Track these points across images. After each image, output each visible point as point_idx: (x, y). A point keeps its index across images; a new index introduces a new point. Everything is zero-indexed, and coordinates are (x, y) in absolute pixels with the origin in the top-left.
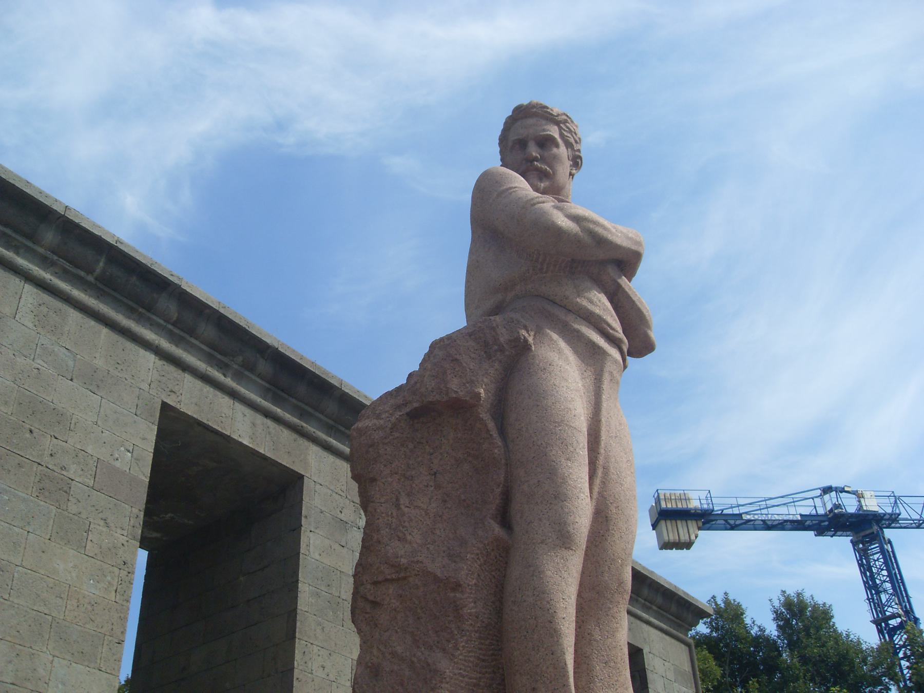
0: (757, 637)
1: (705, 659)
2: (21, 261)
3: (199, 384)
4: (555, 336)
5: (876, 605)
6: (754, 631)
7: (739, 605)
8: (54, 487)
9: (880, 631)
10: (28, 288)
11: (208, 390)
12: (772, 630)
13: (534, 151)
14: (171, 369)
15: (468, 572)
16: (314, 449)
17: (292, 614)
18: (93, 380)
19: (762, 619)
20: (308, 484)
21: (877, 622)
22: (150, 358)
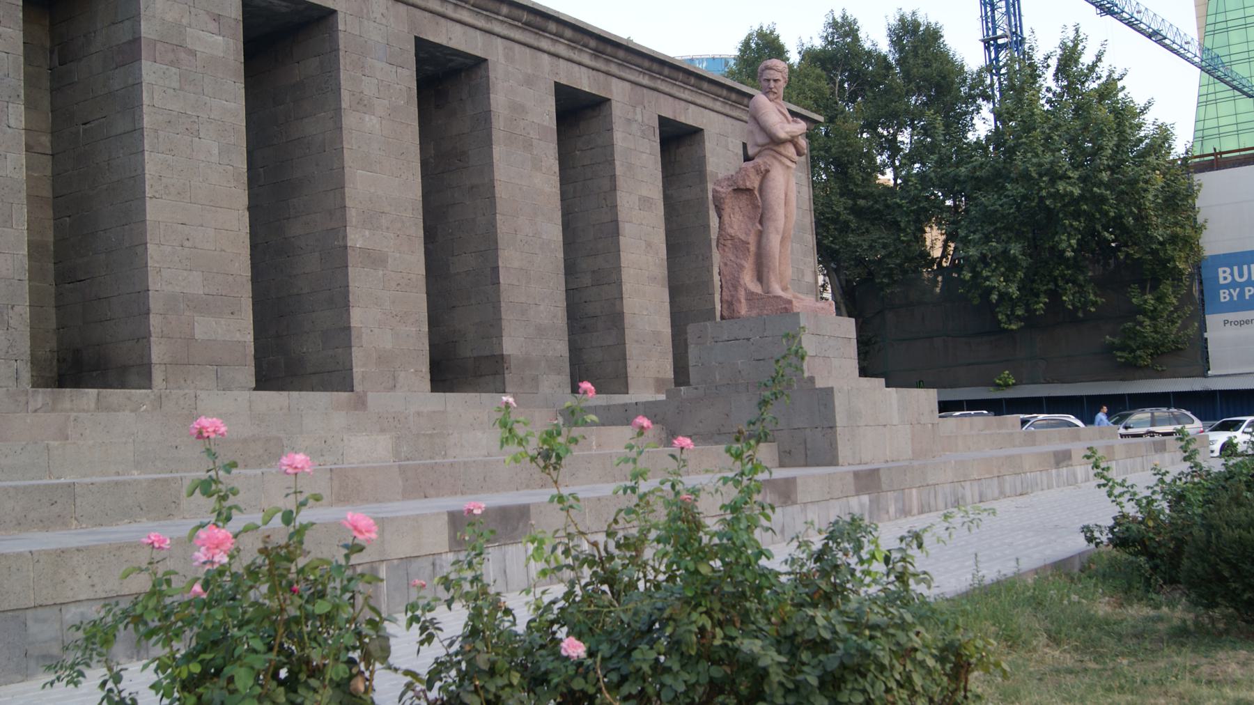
0: (869, 53)
1: (818, 78)
2: (498, 28)
3: (566, 62)
4: (776, 164)
5: (989, 20)
6: (867, 46)
7: (855, 22)
8: (528, 145)
9: (987, 48)
10: (499, 40)
11: (570, 64)
12: (884, 46)
13: (772, 84)
14: (555, 59)
15: (752, 240)
16: (614, 80)
17: (613, 178)
18: (529, 81)
19: (876, 37)
20: (614, 103)
21: (987, 43)
22: (546, 56)
